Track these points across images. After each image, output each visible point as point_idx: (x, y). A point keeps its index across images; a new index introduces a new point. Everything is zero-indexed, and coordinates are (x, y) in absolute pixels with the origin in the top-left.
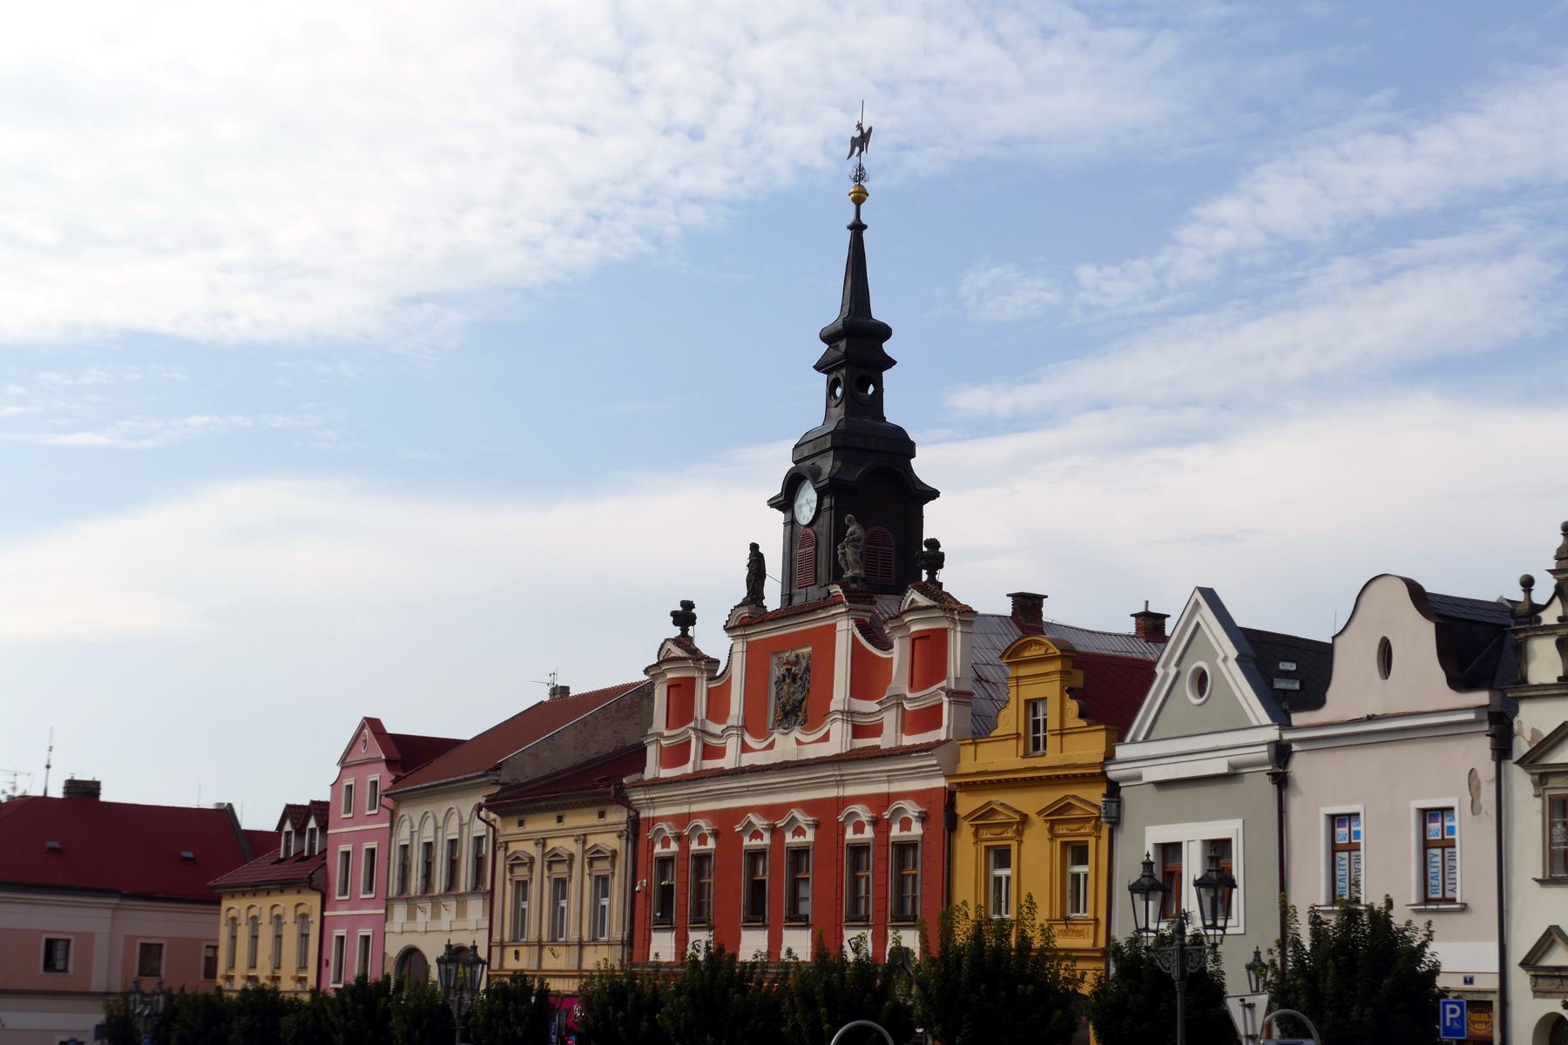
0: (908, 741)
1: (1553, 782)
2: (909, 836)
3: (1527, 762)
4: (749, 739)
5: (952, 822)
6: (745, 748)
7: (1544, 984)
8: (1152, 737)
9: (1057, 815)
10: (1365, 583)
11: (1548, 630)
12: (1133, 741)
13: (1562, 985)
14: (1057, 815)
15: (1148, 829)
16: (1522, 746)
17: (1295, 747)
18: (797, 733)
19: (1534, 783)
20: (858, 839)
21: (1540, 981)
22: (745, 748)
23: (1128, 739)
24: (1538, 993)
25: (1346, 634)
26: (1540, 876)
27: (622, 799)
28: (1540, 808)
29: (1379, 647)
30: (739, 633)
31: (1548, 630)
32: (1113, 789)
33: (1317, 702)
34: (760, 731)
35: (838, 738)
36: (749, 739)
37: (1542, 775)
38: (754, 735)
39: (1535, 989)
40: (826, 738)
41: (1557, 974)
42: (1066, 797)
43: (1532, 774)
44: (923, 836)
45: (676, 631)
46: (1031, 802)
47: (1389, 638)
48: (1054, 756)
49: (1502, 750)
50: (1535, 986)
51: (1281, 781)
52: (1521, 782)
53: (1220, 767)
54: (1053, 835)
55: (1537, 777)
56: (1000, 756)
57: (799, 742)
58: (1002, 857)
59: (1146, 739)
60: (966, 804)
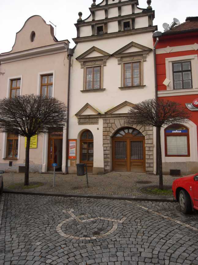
1: (87, 64)
7: (82, 121)
10: (31, 16)
13: (89, 121)
19: (81, 65)
21: (81, 120)
24: (80, 123)
25: (21, 32)
29: (31, 33)
37: (84, 62)
39: (79, 122)
41: (88, 117)
43: (80, 62)
47: (35, 32)
50: (79, 121)
55: (83, 63)
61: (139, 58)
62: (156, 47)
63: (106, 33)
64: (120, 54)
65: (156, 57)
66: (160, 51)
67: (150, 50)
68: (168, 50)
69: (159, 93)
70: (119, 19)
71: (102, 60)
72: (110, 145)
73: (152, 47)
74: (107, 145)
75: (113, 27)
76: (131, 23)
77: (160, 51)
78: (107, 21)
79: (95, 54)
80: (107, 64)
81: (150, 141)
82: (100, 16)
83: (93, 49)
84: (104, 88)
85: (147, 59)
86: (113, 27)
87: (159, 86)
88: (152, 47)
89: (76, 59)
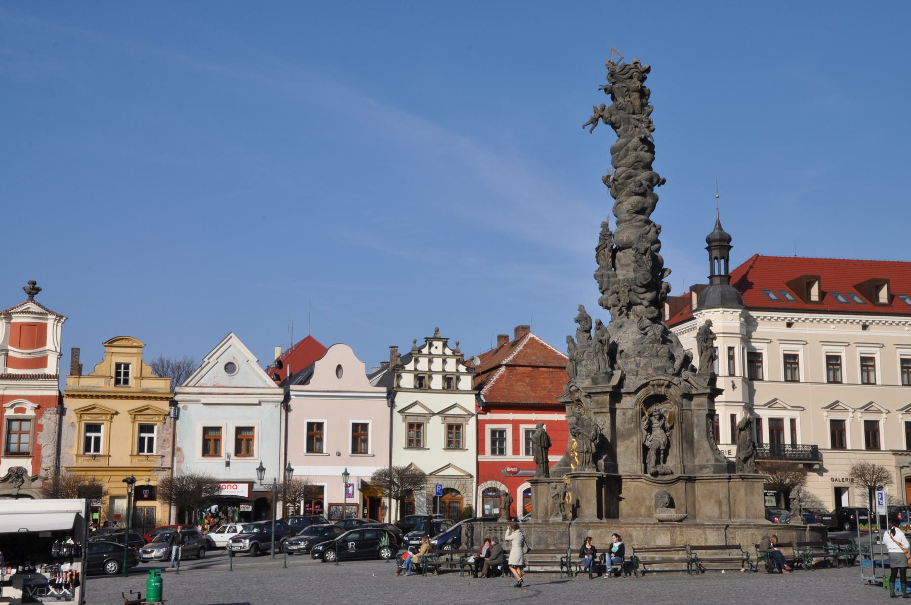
0: (11, 371)
5: (62, 412)
8: (197, 385)
11: (410, 372)
12: (186, 386)
17: (292, 397)
19: (403, 418)
31: (410, 372)
32: (174, 403)
37: (406, 416)
44: (35, 417)
46: (124, 407)
51: (287, 409)
52: (398, 417)
54: (134, 420)
56: (105, 385)
59: (194, 386)
60: (68, 403)
63: (430, 388)
64: (442, 414)
65: (477, 421)
66: (481, 417)
67: (473, 415)
68: (489, 416)
69: (479, 457)
73: (474, 412)
75: (437, 382)
77: (481, 417)
80: (430, 421)
82: (423, 365)
83: (415, 403)
84: (427, 447)
85: (469, 422)
86: (437, 382)
87: (480, 450)
88: (474, 412)
89: (399, 412)
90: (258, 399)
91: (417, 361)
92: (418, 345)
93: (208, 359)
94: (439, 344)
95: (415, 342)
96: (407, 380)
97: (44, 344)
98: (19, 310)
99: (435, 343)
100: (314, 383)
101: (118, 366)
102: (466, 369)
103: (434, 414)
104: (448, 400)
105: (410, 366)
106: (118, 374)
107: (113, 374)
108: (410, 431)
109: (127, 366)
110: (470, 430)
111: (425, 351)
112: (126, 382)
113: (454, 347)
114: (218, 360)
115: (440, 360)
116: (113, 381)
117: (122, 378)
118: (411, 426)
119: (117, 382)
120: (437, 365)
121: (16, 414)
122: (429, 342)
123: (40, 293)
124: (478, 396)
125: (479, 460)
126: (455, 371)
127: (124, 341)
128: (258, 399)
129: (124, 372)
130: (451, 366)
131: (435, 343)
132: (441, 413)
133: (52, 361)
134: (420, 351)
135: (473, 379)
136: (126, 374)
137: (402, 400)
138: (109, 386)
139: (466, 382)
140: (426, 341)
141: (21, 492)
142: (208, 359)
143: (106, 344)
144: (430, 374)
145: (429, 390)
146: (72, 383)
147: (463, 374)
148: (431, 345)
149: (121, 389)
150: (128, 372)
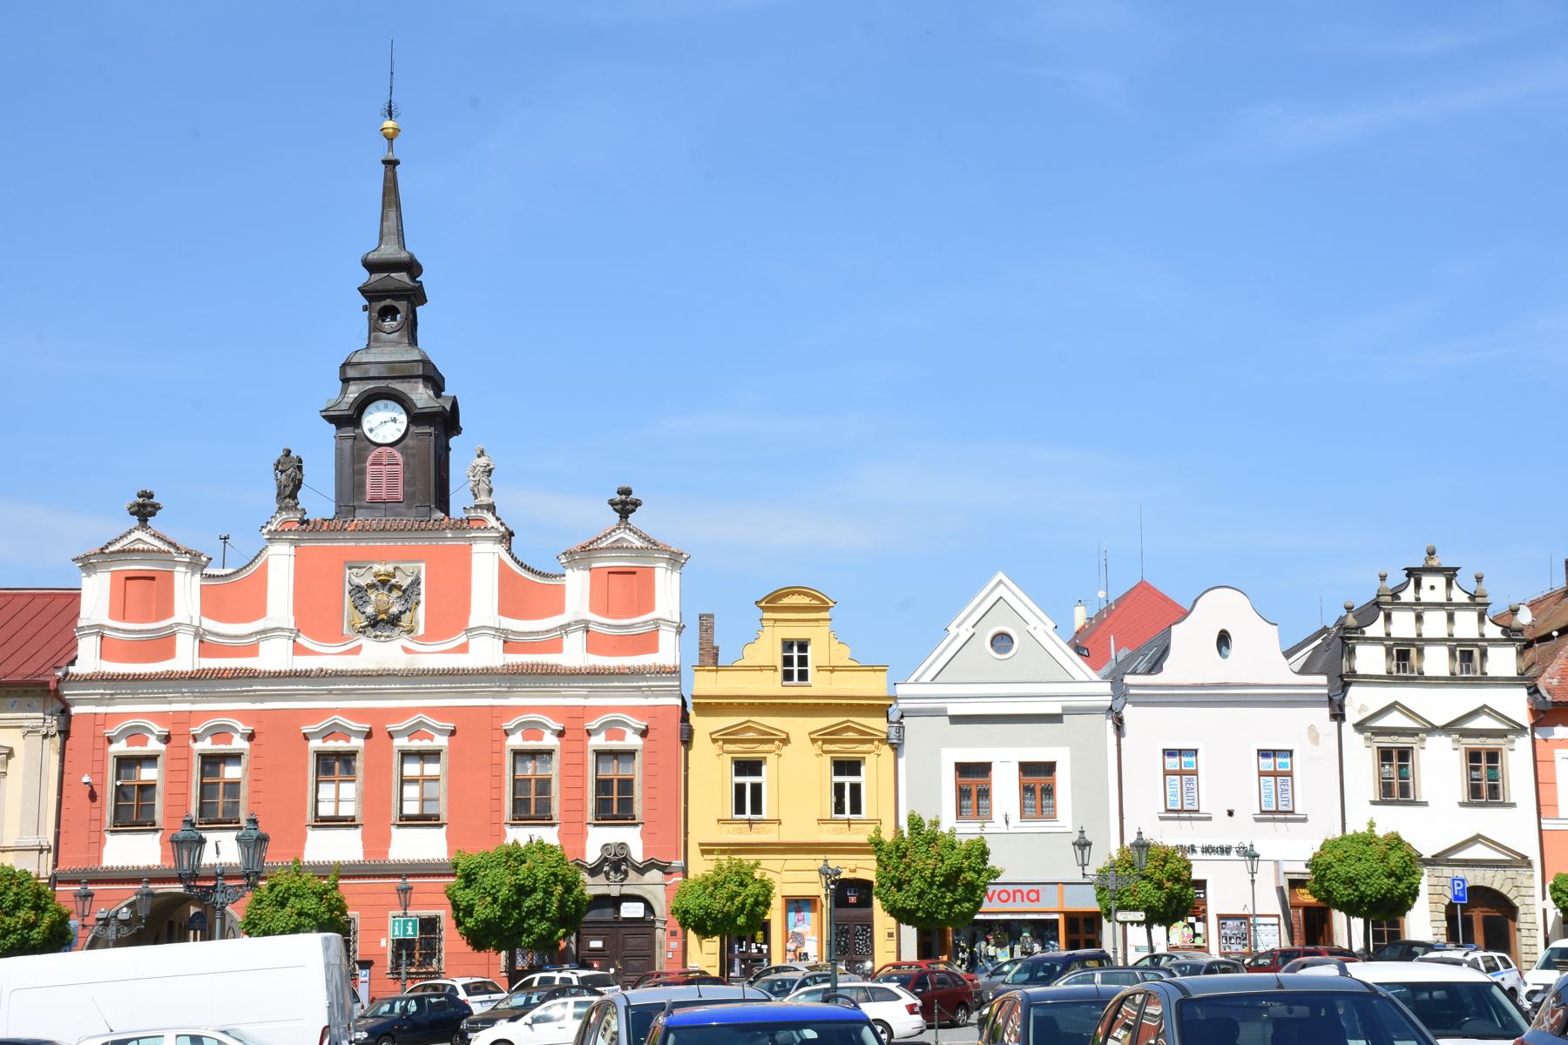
2: (624, 746)
3: (1360, 727)
4: (303, 641)
5: (687, 739)
6: (299, 650)
8: (937, 680)
9: (824, 738)
11: (1375, 640)
12: (916, 682)
14: (824, 738)
15: (1067, 750)
16: (1353, 714)
18: (404, 641)
20: (530, 746)
22: (299, 650)
23: (912, 680)
26: (1373, 800)
27: (57, 694)
28: (1371, 755)
30: (292, 537)
31: (1375, 640)
33: (1155, 667)
34: (329, 633)
35: (486, 654)
36: (303, 641)
38: (313, 635)
40: (463, 649)
42: (848, 721)
45: (135, 521)
46: (799, 728)
48: (819, 685)
49: (1338, 716)
52: (1354, 741)
53: (1054, 708)
57: (406, 650)
58: (748, 767)
61: (1500, 741)
62: (1533, 726)
67: (1519, 730)
70: (1450, 641)
71: (1417, 735)
72: (1445, 924)
74: (1439, 924)
75: (1436, 661)
76: (1476, 652)
78: (1420, 643)
79: (1395, 720)
81: (1529, 918)
82: (1403, 625)
86: (1436, 661)
90: (1060, 704)
91: (1388, 618)
92: (1391, 583)
93: (958, 626)
94: (1440, 581)
95: (1383, 578)
96: (1370, 659)
97: (650, 607)
98: (604, 545)
99: (1427, 581)
100: (1173, 671)
101: (788, 645)
102: (1503, 632)
103: (1433, 730)
104: (1468, 699)
105: (1376, 629)
106: (788, 661)
107: (779, 663)
108: (1383, 766)
109: (803, 646)
110: (1517, 760)
111: (1408, 595)
112: (803, 676)
113: (1472, 587)
114: (972, 631)
115: (1443, 615)
116: (779, 675)
117: (796, 668)
118: (1385, 755)
119: (788, 676)
120: (1435, 624)
121: (609, 743)
122: (1414, 574)
123: (639, 509)
124: (1534, 691)
125: (1543, 827)
126: (1477, 636)
127: (795, 597)
128: (1060, 704)
129: (799, 657)
130: (1466, 627)
131: (1427, 581)
132: (1447, 729)
133: (667, 638)
134: (1395, 595)
135: (1520, 653)
136: (803, 661)
137: (1360, 701)
138: (771, 685)
139: (1503, 661)
140: (1409, 575)
141: (627, 890)
142: (958, 626)
143: (763, 604)
144: (1420, 643)
145: (1421, 680)
146: (707, 684)
147: (1494, 642)
148: (1418, 585)
149: (795, 689)
150: (806, 657)
